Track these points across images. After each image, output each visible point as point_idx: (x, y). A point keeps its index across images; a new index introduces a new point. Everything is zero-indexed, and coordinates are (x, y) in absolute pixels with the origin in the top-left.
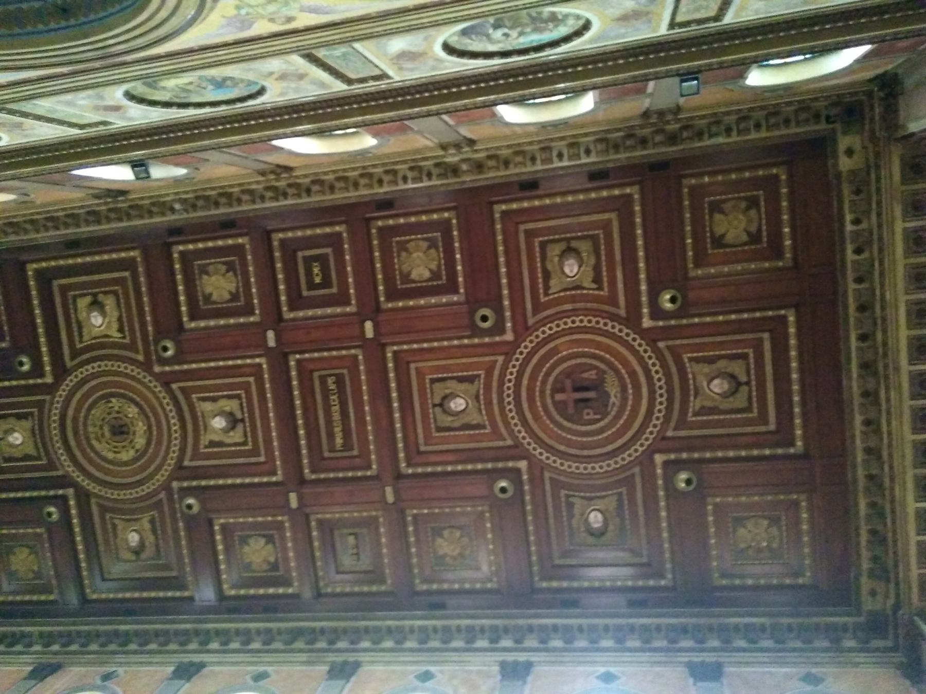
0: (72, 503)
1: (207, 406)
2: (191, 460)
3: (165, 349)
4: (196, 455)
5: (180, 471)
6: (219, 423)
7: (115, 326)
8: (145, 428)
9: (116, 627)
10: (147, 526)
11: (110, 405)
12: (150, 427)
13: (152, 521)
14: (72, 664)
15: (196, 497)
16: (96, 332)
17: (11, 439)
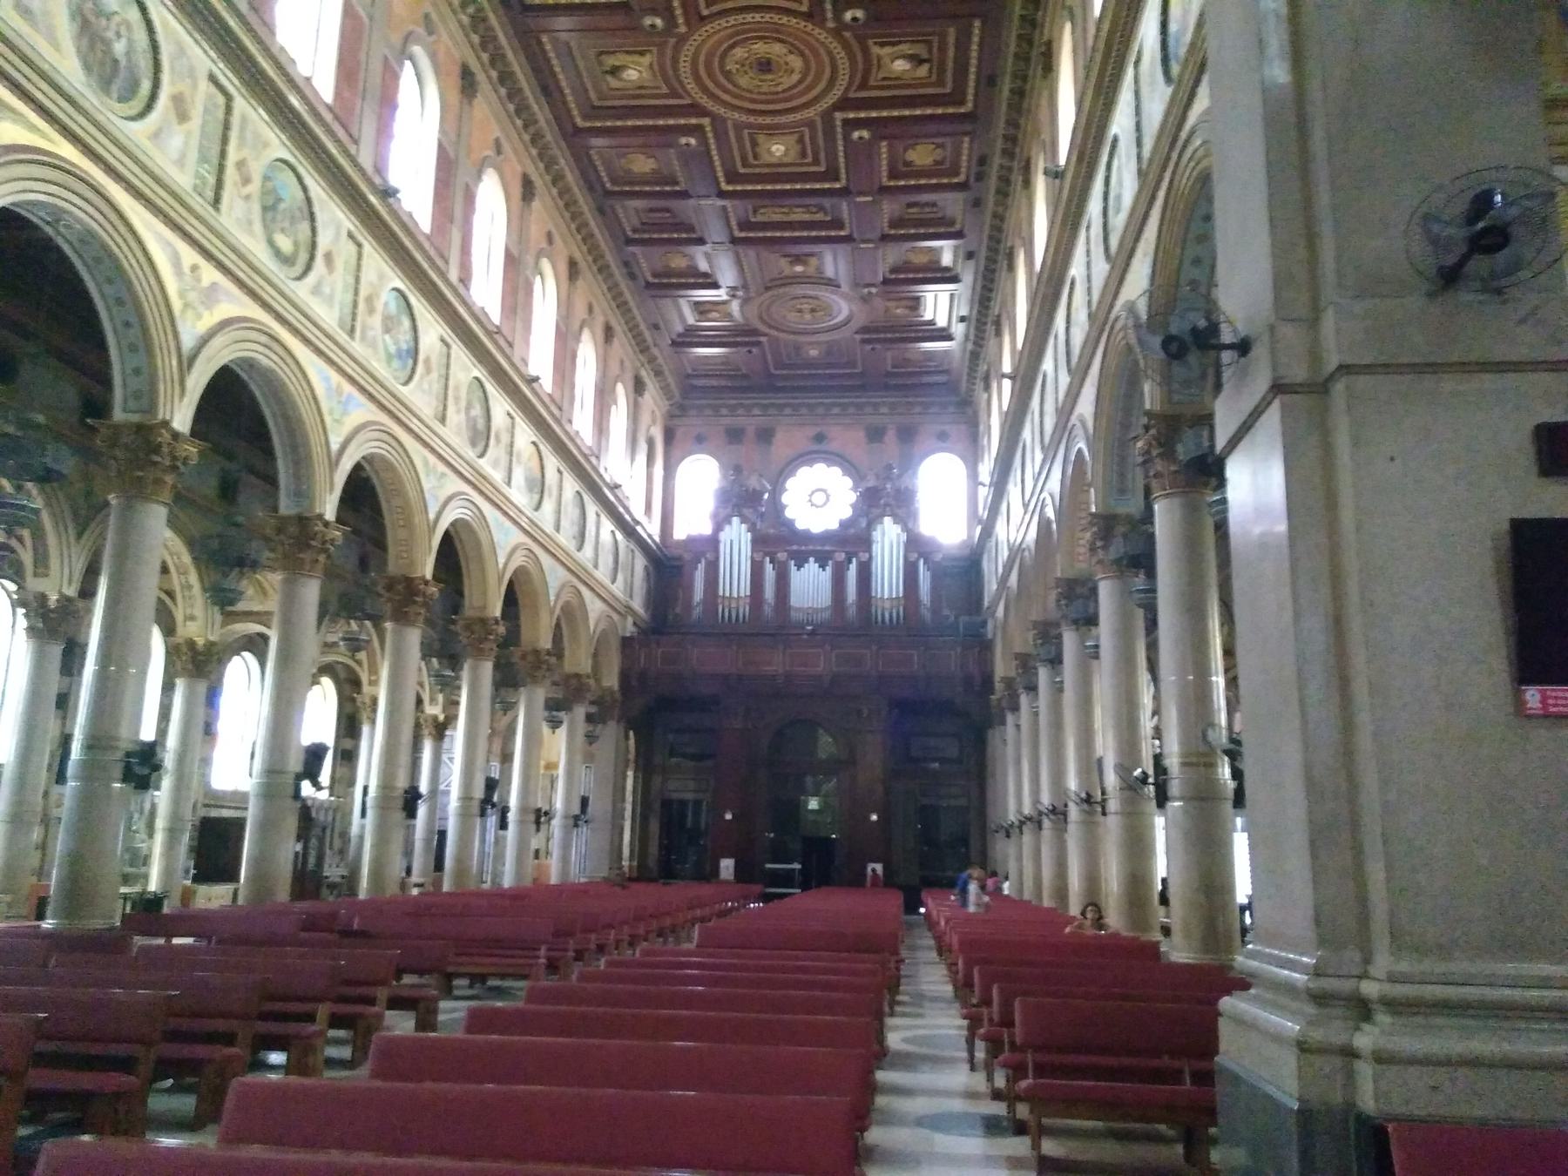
0: (851, 115)
7: (636, 58)
10: (887, 50)
13: (882, 45)
17: (782, 148)
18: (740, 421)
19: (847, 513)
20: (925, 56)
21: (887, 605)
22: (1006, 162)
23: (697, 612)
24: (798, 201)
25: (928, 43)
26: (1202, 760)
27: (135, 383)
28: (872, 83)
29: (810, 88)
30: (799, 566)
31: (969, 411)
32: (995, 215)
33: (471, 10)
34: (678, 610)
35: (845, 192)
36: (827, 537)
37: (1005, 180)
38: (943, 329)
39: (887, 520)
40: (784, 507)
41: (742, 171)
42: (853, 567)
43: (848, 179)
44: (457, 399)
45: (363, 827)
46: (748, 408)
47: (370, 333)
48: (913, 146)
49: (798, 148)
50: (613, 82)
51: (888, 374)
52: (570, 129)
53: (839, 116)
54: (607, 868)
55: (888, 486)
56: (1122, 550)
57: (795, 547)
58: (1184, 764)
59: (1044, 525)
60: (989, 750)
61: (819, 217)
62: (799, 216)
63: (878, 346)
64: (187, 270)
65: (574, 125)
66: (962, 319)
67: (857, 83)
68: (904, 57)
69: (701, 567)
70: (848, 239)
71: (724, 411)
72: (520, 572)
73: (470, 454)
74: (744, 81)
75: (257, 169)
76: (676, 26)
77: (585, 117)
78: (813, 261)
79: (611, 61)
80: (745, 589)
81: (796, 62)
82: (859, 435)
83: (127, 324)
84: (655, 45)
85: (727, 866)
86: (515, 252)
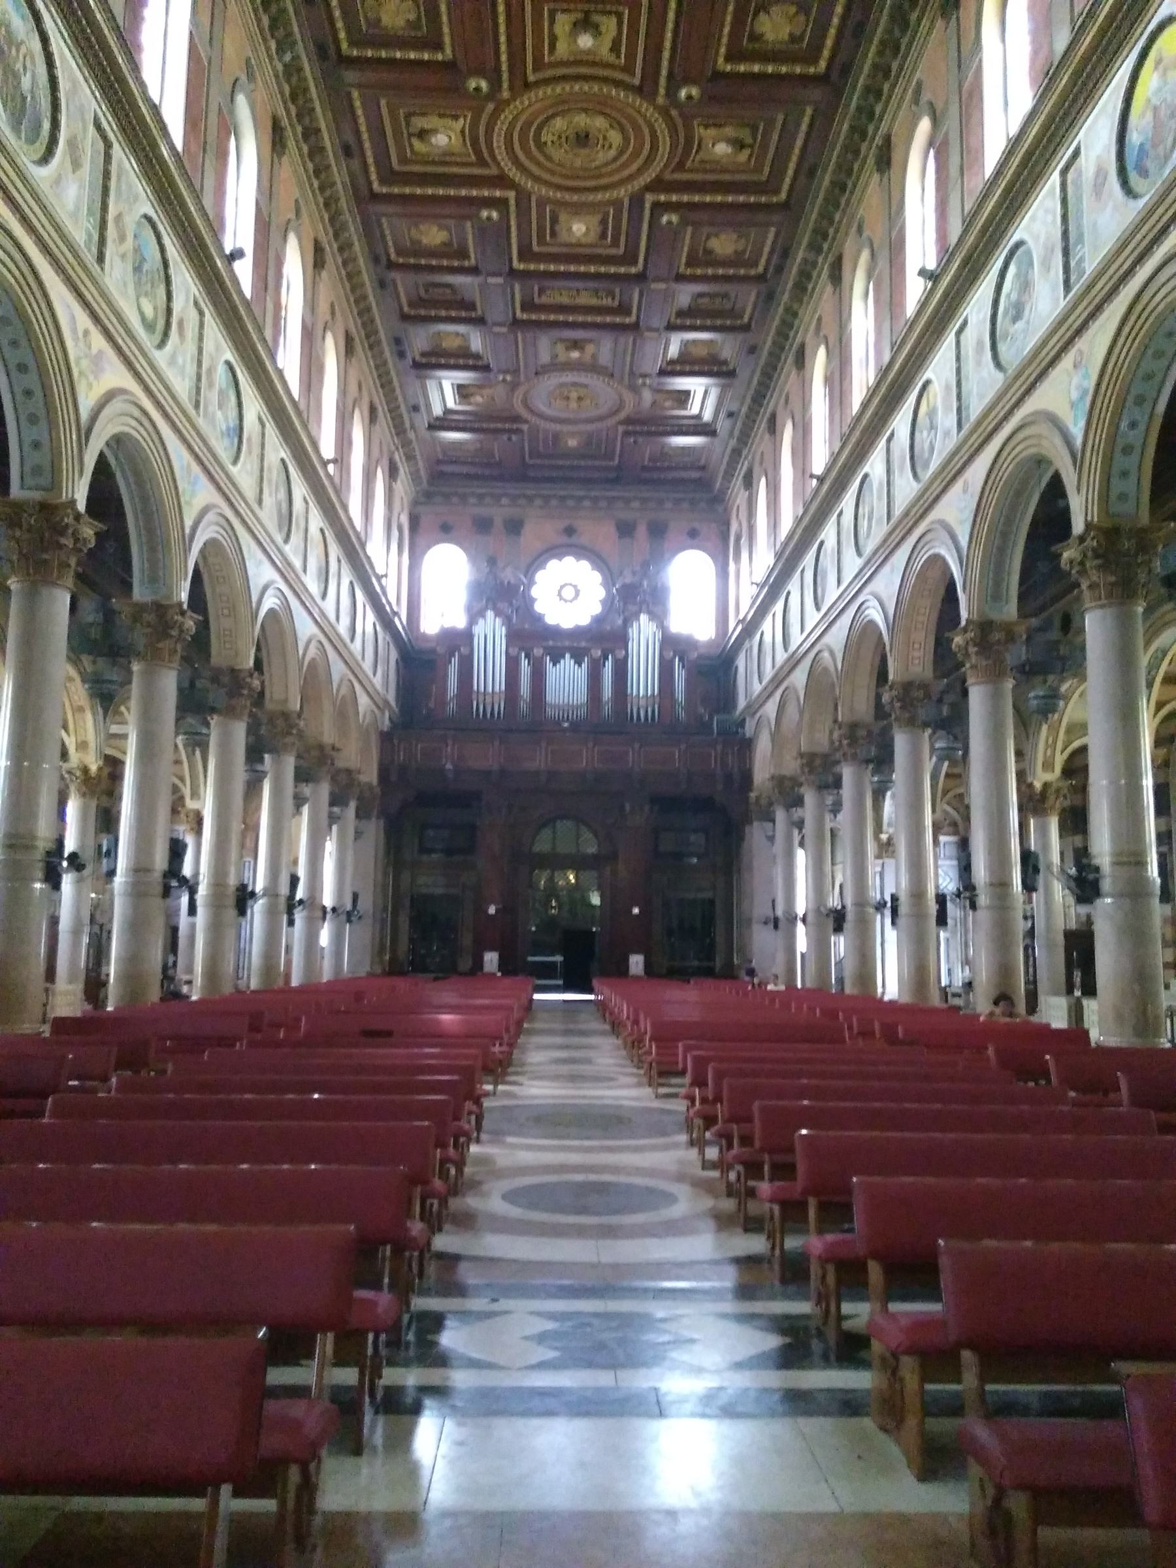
0: (662, 198)
1: (562, 48)
2: (633, 74)
3: (478, 89)
4: (629, 69)
5: (645, 90)
6: (585, 41)
7: (449, 122)
8: (584, 115)
10: (712, 132)
11: (549, 143)
13: (706, 127)
14: (842, 244)
15: (679, 88)
16: (456, 141)
18: (483, 511)
19: (597, 609)
20: (749, 140)
21: (642, 703)
22: (811, 256)
23: (452, 706)
24: (591, 284)
25: (754, 129)
26: (1132, 859)
28: (689, 164)
29: (625, 166)
30: (555, 662)
31: (720, 509)
32: (787, 310)
33: (288, 57)
34: (432, 705)
35: (641, 277)
36: (577, 633)
37: (805, 275)
38: (707, 425)
39: (644, 618)
40: (533, 600)
42: (609, 664)
44: (270, 481)
45: (193, 927)
47: (210, 409)
49: (599, 229)
51: (644, 468)
52: (365, 192)
53: (649, 198)
54: (368, 962)
55: (645, 583)
56: (1024, 657)
57: (551, 643)
58: (1116, 864)
59: (864, 633)
60: (745, 845)
61: (607, 302)
62: (585, 299)
63: (640, 440)
64: (80, 335)
65: (371, 190)
66: (730, 415)
67: (673, 165)
69: (455, 661)
70: (635, 327)
71: (472, 500)
72: (313, 664)
73: (279, 539)
74: (557, 154)
75: (131, 221)
77: (383, 181)
78: (590, 349)
79: (420, 123)
80: (500, 685)
81: (615, 137)
83: (28, 393)
84: (469, 109)
85: (491, 959)
86: (309, 325)
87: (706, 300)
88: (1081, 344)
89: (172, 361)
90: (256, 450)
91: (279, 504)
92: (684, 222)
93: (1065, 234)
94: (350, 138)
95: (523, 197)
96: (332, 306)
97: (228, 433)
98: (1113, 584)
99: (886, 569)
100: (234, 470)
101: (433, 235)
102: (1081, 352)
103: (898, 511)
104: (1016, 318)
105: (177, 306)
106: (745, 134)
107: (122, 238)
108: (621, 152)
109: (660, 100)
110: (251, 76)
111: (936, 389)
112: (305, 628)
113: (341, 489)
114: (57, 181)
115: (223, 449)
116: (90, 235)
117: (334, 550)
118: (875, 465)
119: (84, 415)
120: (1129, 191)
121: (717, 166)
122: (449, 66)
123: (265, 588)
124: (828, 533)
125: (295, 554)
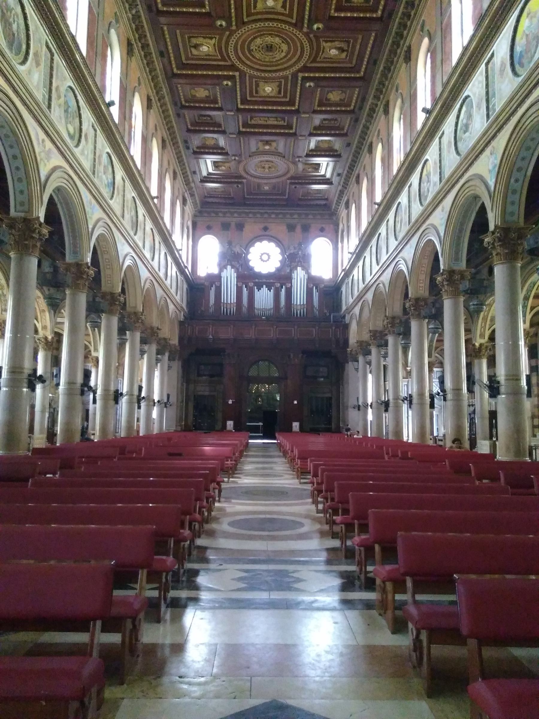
2: (292, 18)
3: (221, 25)
4: (290, 16)
5: (298, 25)
8: (270, 37)
9: (380, 71)
10: (329, 44)
11: (254, 50)
12: (270, 34)
13: (326, 42)
14: (389, 95)
17: (270, 89)
18: (227, 219)
19: (278, 265)
21: (299, 308)
22: (375, 102)
23: (211, 310)
24: (274, 115)
25: (348, 42)
26: (514, 378)
27: (20, 198)
29: (290, 59)
30: (259, 289)
33: (134, 12)
34: (203, 309)
35: (297, 112)
36: (269, 276)
37: (373, 110)
38: (328, 179)
39: (299, 269)
40: (249, 261)
41: (249, 99)
42: (283, 290)
43: (299, 106)
44: (127, 207)
45: (95, 409)
46: (232, 213)
47: (100, 175)
48: (331, 92)
49: (277, 89)
50: (195, 52)
51: (300, 200)
52: (170, 74)
53: (300, 75)
54: (174, 426)
56: (468, 287)
57: (257, 280)
58: (506, 380)
59: (398, 275)
61: (282, 123)
62: (272, 122)
65: (173, 72)
66: (339, 175)
67: (311, 60)
68: (336, 48)
69: (213, 289)
70: (295, 134)
71: (220, 215)
73: (132, 234)
74: (257, 55)
75: (63, 89)
76: (231, 26)
77: (178, 69)
78: (274, 144)
79: (194, 41)
80: (234, 299)
81: (285, 47)
82: (284, 228)
83: (17, 168)
84: (218, 34)
85: (230, 424)
86: (145, 135)
87: (327, 122)
88: (494, 143)
89: (82, 153)
90: (121, 193)
91: (132, 217)
92: (317, 86)
93: (487, 93)
94: (163, 49)
95: (243, 75)
96: (156, 126)
97: (108, 185)
98: (506, 253)
99: (408, 246)
100: (111, 202)
101: (201, 93)
102: (493, 147)
103: (413, 220)
104: (465, 132)
105: (84, 128)
106: (343, 45)
107: (59, 97)
108: (288, 53)
109: (305, 30)
110: (117, 21)
111: (430, 163)
112: (144, 274)
113: (160, 211)
114: (29, 72)
115: (106, 192)
116: (44, 96)
117: (157, 238)
118: (403, 199)
119: (43, 178)
120: (515, 73)
121: (331, 60)
122: (208, 14)
123: (126, 256)
124: (383, 230)
125: (139, 240)
